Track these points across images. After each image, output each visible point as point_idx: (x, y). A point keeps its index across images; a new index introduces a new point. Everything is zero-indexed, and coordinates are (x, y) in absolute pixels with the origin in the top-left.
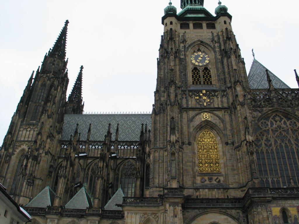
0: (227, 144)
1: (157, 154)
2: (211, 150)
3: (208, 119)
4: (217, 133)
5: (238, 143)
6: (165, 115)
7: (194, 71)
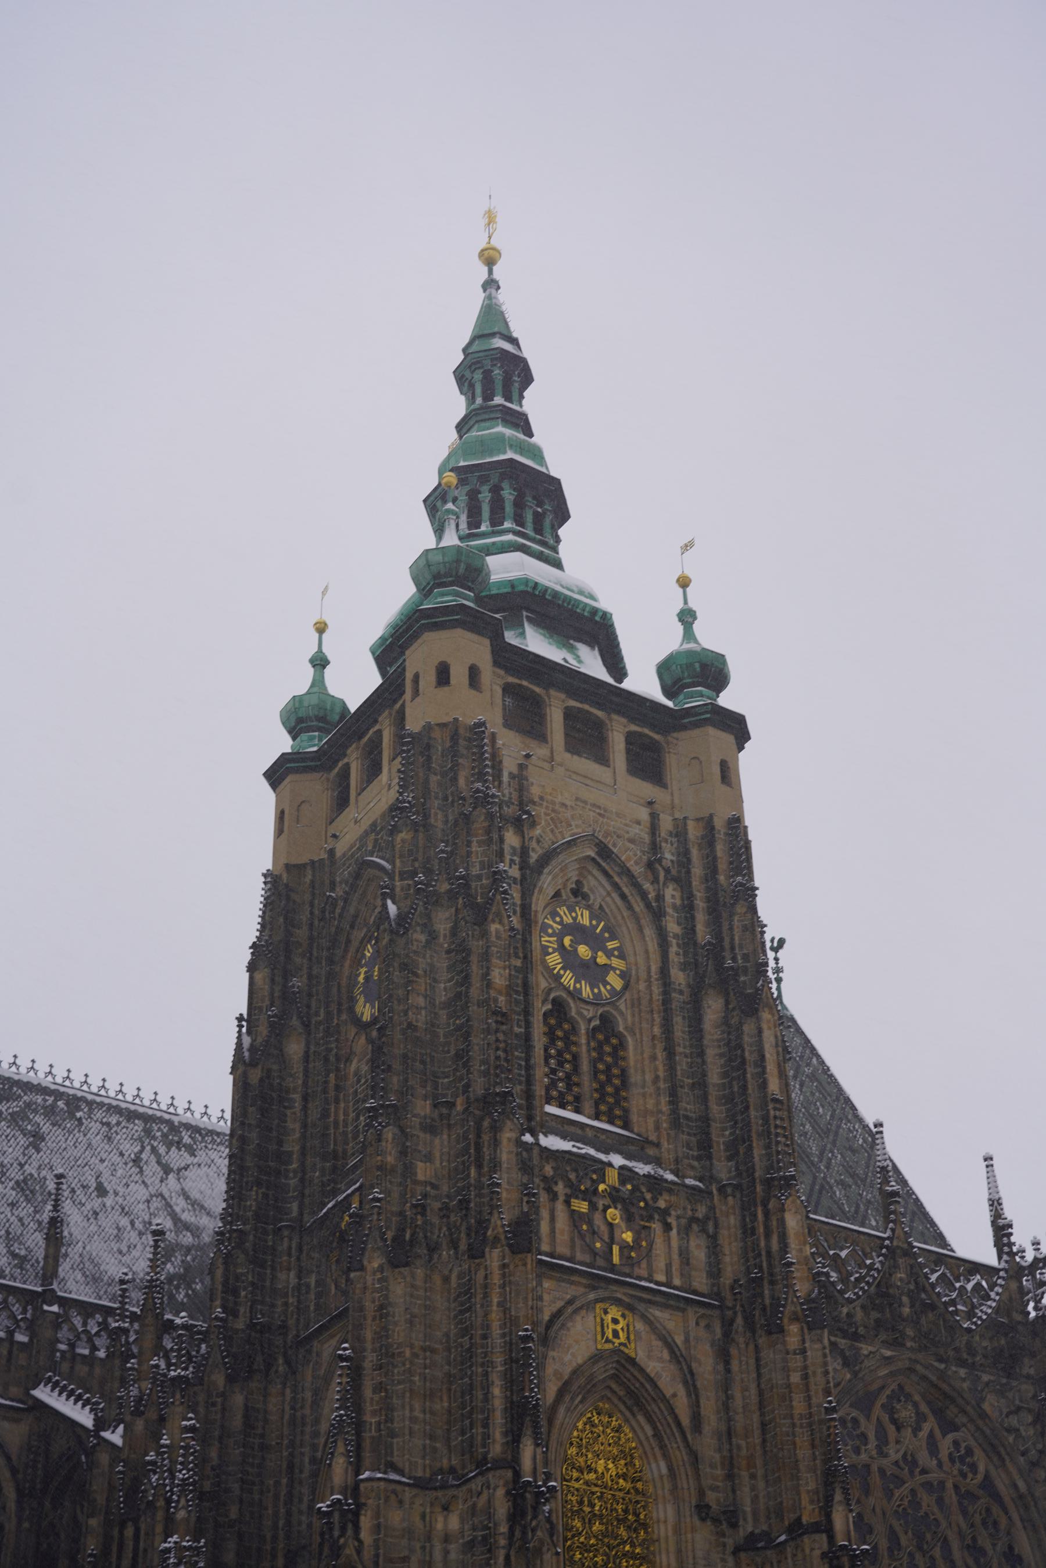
0: (702, 1510)
1: (395, 1518)
2: (622, 1532)
3: (625, 1345)
4: (657, 1435)
5: (756, 1520)
6: (437, 1279)
7: (553, 1022)
